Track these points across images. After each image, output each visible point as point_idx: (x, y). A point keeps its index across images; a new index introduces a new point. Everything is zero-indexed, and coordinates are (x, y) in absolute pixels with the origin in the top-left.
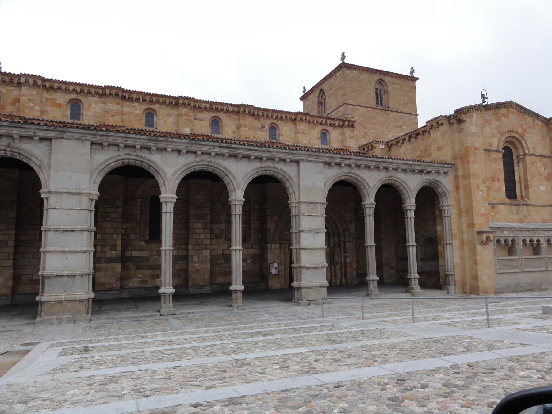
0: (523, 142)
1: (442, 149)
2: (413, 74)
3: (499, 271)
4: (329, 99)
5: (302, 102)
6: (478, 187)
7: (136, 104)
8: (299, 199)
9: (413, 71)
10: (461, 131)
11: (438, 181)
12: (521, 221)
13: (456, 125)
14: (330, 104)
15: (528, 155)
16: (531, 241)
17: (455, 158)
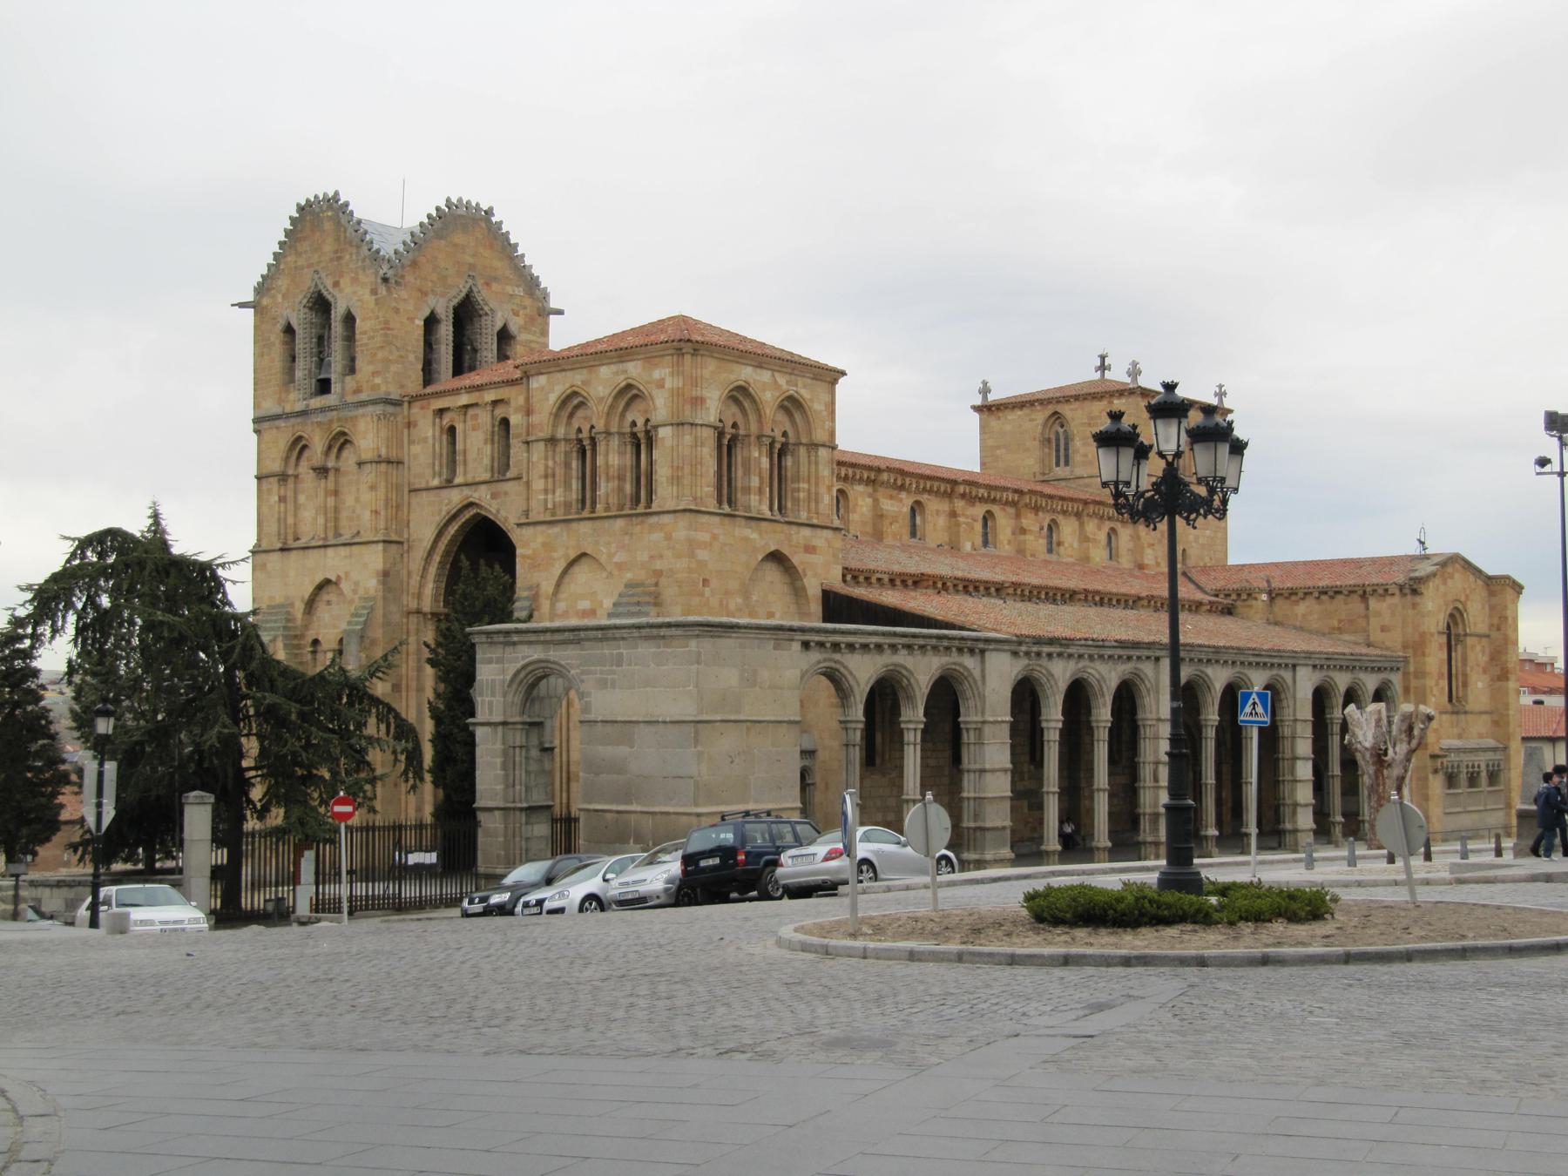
0: (1465, 615)
1: (1389, 631)
2: (1221, 401)
3: (1447, 811)
4: (1084, 445)
5: (976, 416)
6: (1432, 691)
7: (903, 495)
8: (1294, 715)
9: (1221, 394)
10: (1414, 606)
11: (1390, 681)
12: (1460, 737)
13: (1409, 597)
14: (1086, 455)
15: (1471, 635)
16: (1473, 767)
17: (1405, 647)
